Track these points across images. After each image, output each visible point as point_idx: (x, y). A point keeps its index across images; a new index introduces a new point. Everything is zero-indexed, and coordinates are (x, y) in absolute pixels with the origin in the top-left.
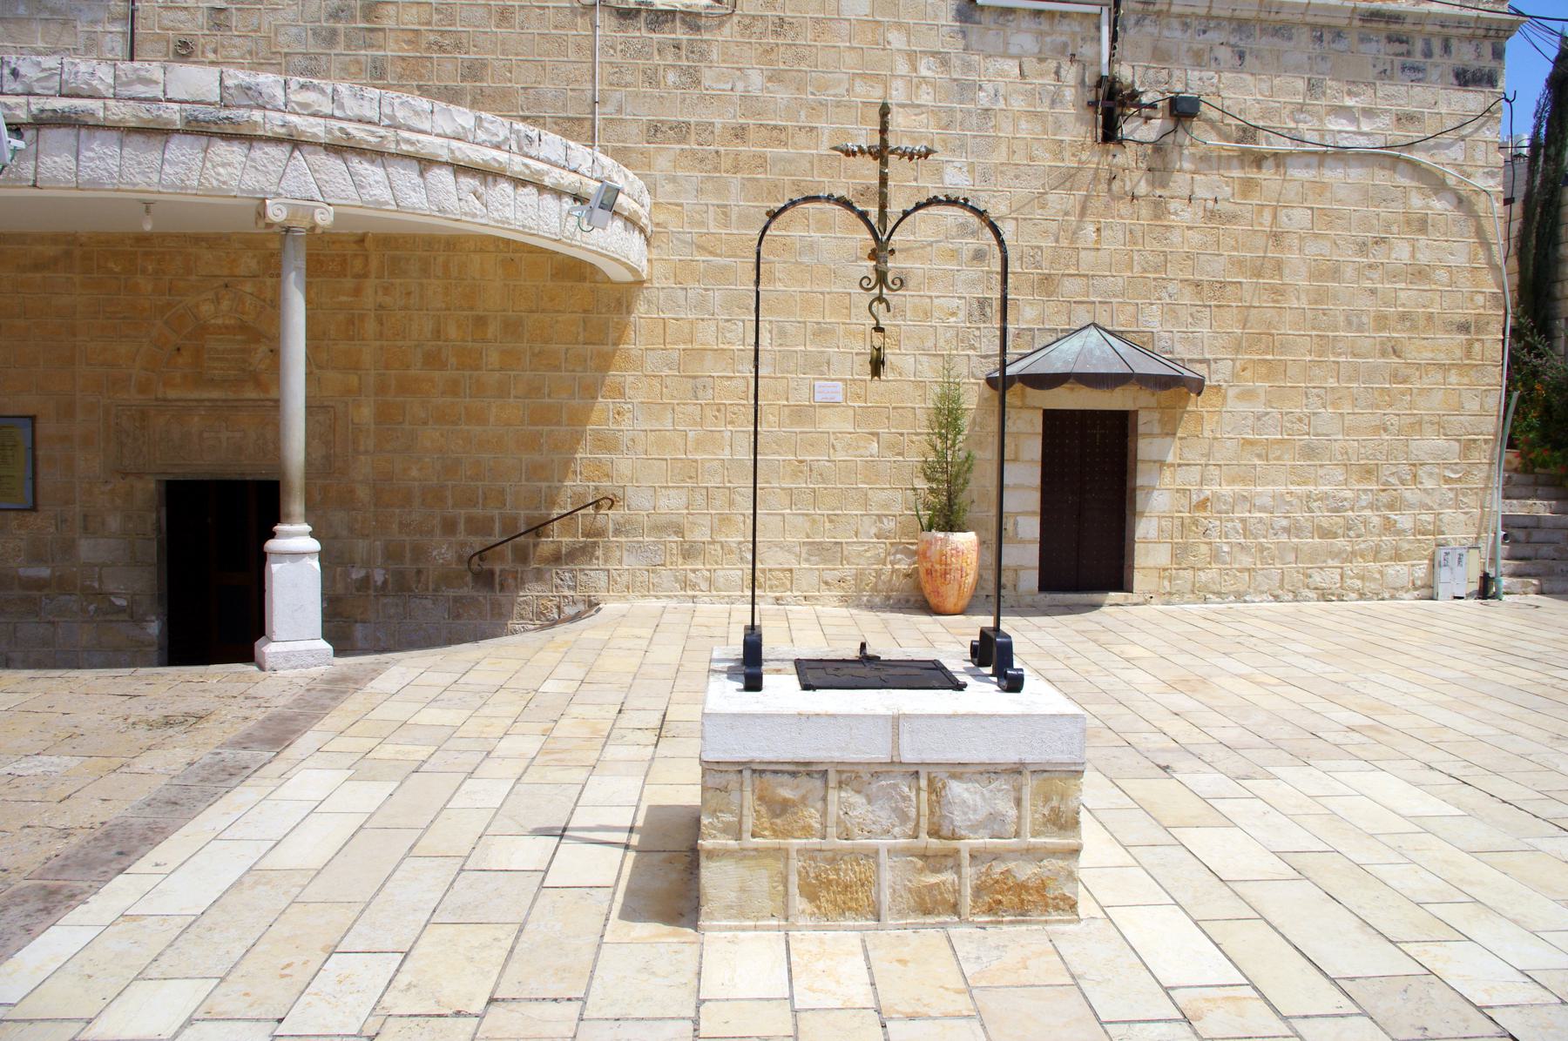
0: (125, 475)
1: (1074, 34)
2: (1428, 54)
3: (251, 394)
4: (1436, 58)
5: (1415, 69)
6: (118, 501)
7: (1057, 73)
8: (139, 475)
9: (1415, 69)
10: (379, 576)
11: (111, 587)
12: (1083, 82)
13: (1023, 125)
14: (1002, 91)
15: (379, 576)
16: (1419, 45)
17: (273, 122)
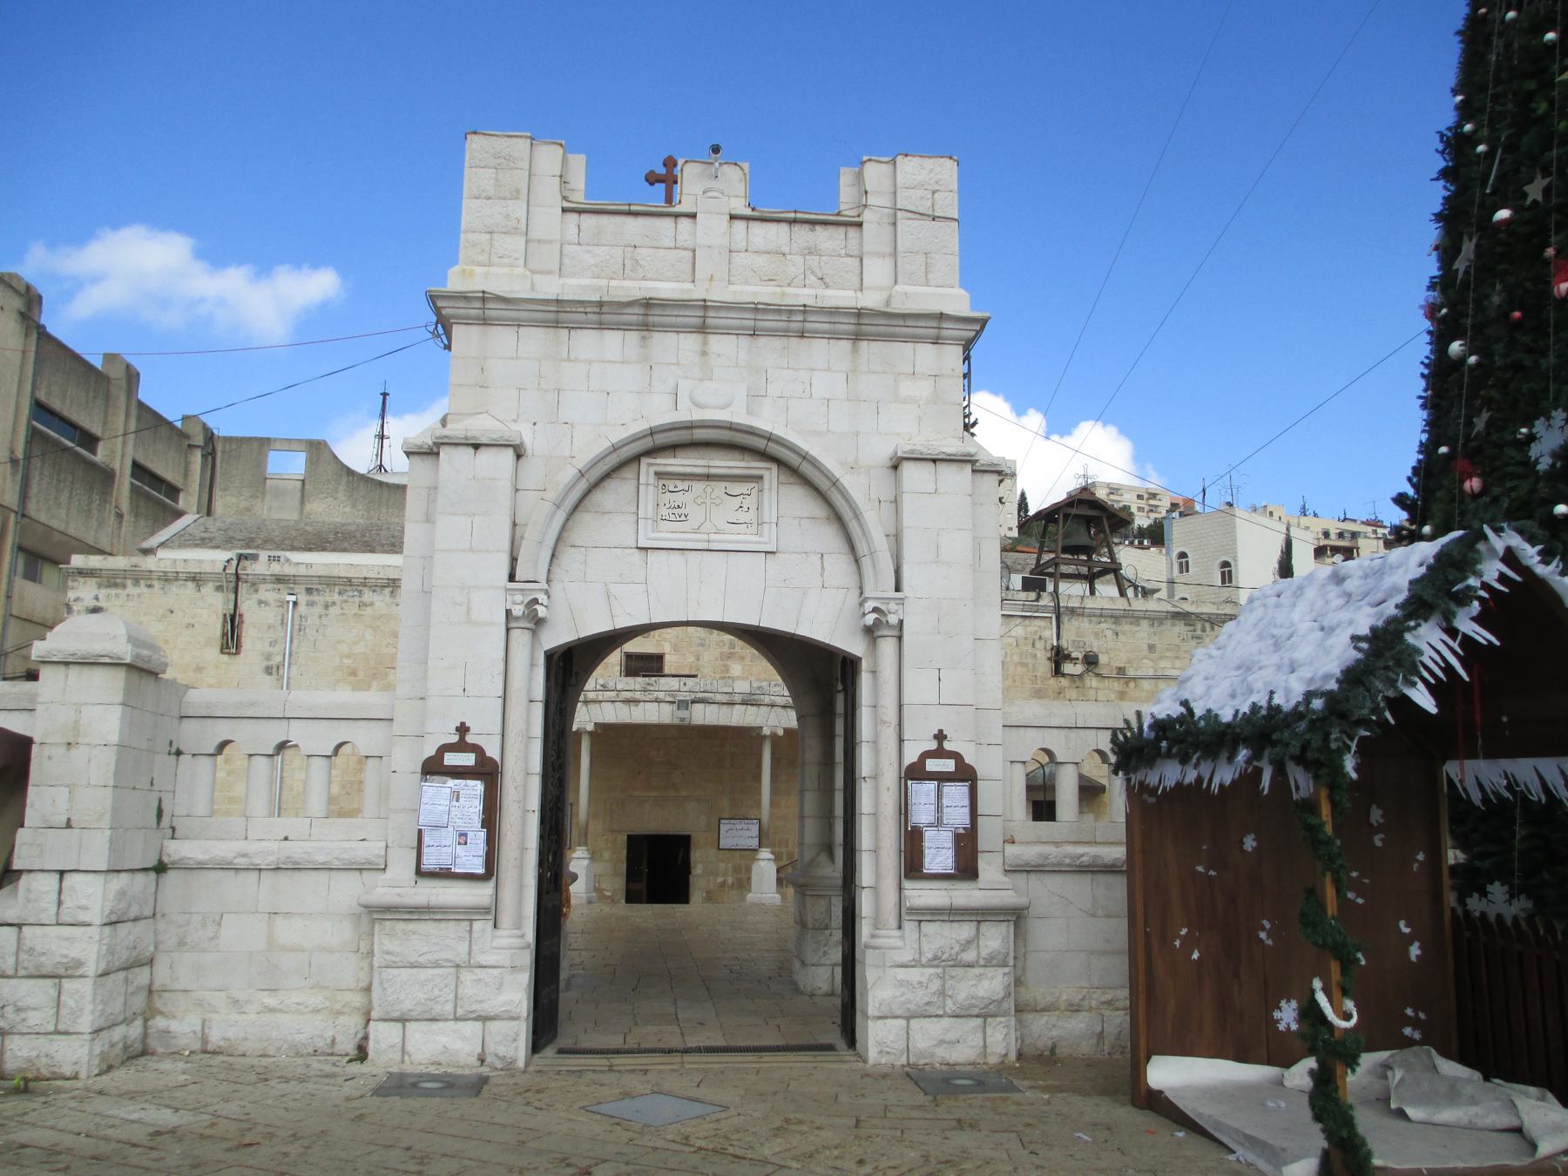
0: (613, 831)
1: (1039, 627)
2: (1204, 630)
3: (672, 793)
4: (1208, 632)
5: (1198, 638)
6: (609, 845)
7: (1033, 644)
8: (620, 831)
9: (1198, 638)
10: (730, 881)
11: (604, 886)
12: (1045, 648)
13: (1019, 668)
14: (1009, 654)
15: (730, 881)
16: (1199, 626)
17: (767, 699)
